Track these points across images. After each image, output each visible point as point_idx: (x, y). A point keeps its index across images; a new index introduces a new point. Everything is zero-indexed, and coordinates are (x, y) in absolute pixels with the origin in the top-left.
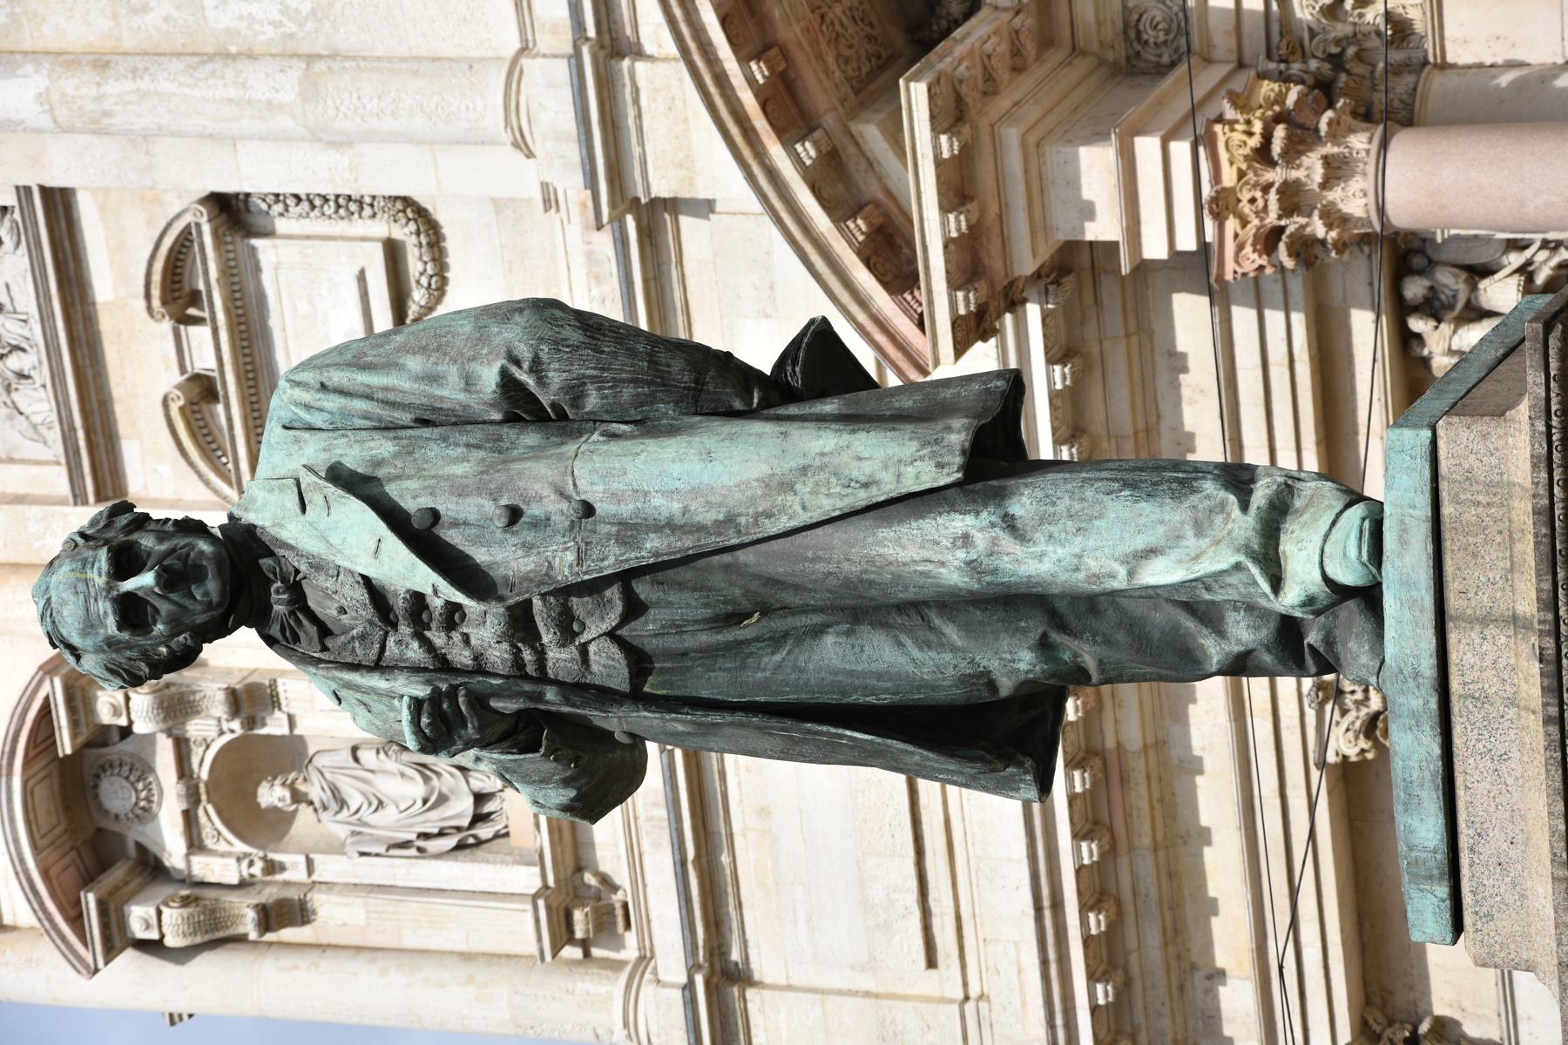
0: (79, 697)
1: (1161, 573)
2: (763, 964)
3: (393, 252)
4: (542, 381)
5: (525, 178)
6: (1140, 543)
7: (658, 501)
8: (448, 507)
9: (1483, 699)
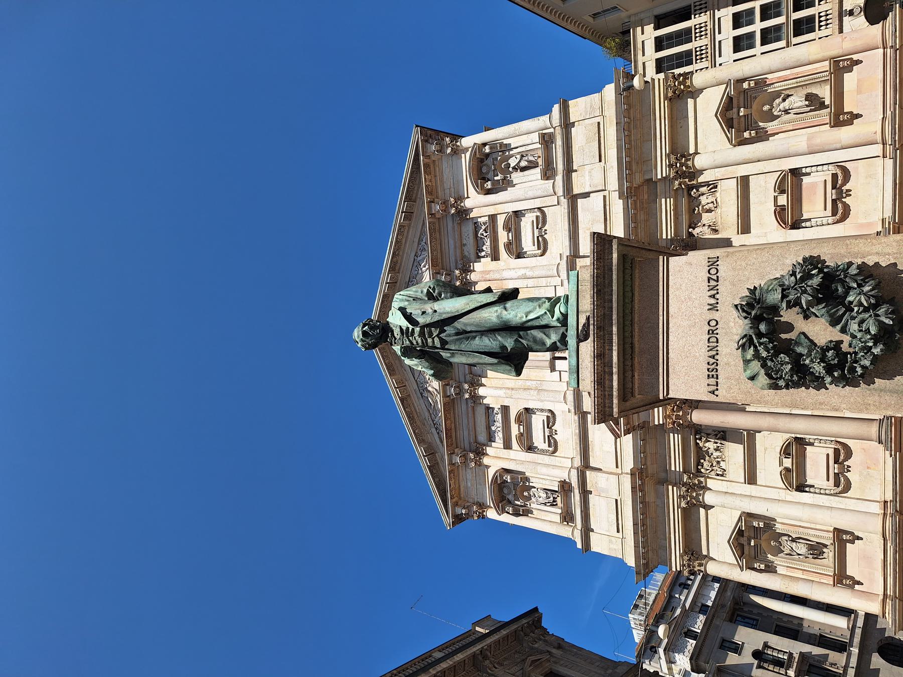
0: (501, 476)
1: (531, 316)
3: (548, 417)
5: (566, 407)
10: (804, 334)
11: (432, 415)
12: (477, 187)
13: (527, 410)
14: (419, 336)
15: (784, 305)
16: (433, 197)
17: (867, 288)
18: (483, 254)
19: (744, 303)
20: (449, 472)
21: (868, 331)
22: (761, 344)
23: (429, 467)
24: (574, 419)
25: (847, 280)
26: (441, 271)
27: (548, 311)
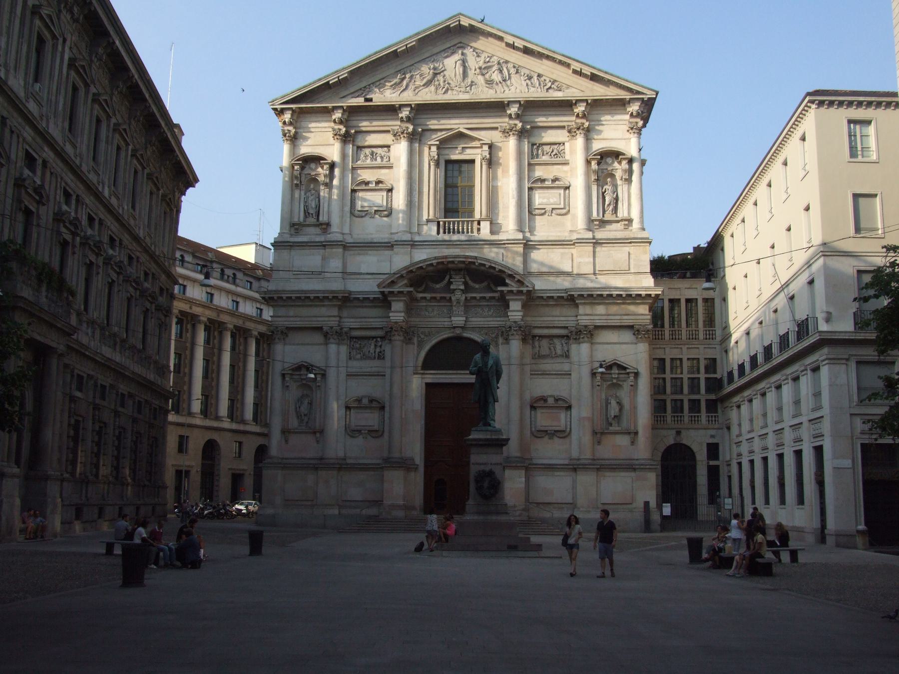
1: (490, 414)
12: (594, 155)
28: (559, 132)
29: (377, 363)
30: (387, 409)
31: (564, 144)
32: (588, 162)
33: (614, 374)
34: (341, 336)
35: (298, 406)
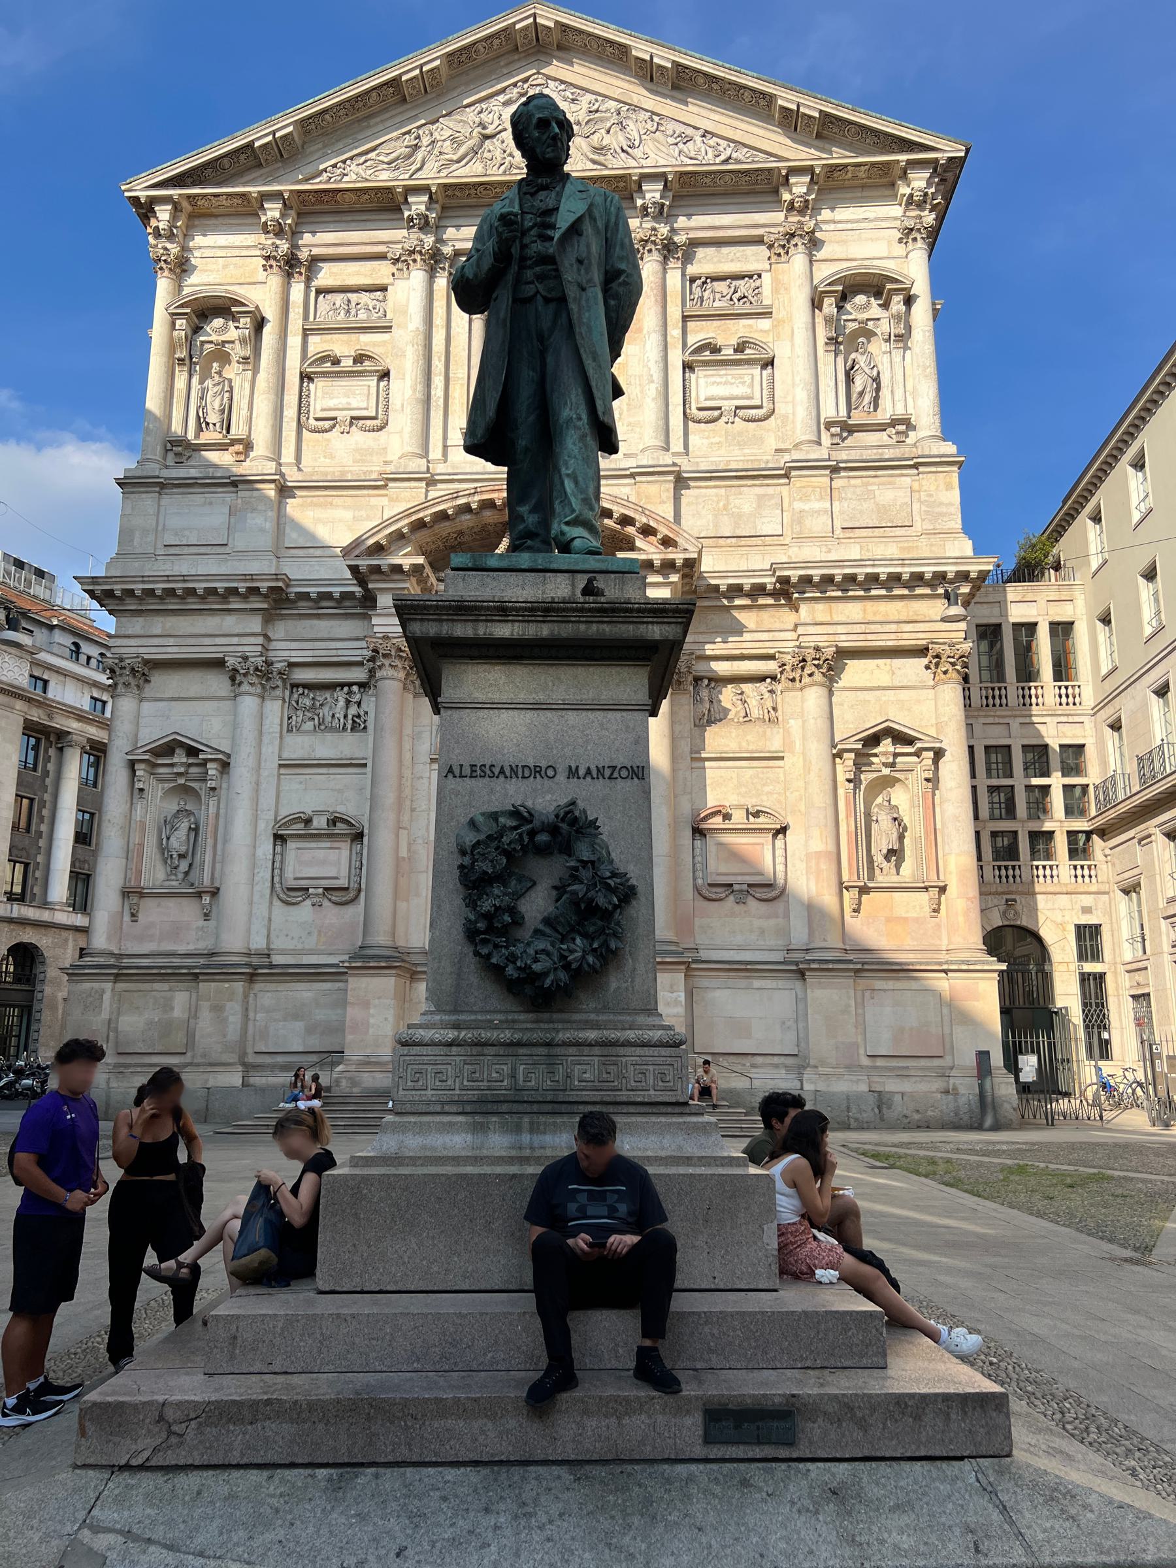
1: (569, 485)
2: (166, 500)
4: (620, 284)
6: (580, 479)
7: (587, 314)
8: (583, 240)
9: (544, 584)
10: (535, 884)
11: (363, 159)
12: (829, 284)
13: (385, 375)
14: (538, 253)
15: (572, 864)
16: (821, 182)
17: (590, 959)
18: (697, 291)
19: (577, 813)
20: (243, 195)
21: (536, 961)
22: (521, 835)
23: (250, 145)
24: (373, 469)
25: (602, 938)
26: (670, 194)
27: (577, 517)
28: (750, 250)
29: (350, 738)
30: (366, 839)
31: (760, 276)
32: (816, 303)
33: (885, 753)
34: (269, 679)
35: (164, 836)
